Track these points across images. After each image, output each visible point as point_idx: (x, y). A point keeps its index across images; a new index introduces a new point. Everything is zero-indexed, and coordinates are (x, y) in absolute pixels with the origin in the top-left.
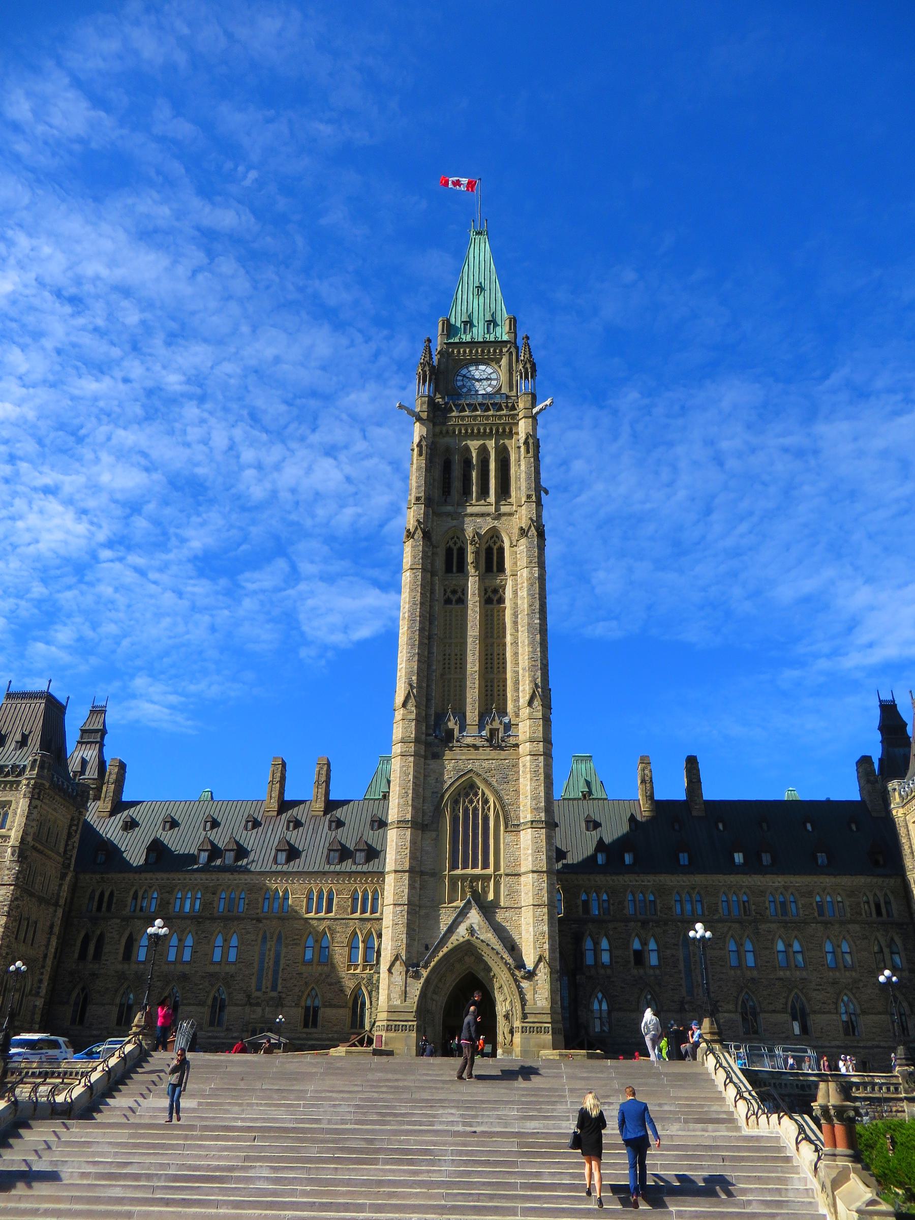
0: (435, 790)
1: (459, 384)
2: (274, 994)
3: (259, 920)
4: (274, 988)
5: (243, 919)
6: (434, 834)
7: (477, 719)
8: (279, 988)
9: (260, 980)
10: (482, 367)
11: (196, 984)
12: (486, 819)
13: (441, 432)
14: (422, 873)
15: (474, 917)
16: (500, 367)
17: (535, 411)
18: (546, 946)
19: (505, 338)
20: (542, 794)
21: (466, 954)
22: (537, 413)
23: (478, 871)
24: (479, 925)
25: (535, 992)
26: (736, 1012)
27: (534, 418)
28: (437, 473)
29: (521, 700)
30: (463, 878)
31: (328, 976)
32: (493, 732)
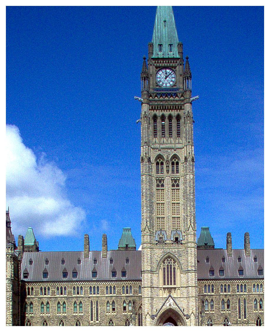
1: (159, 80)
2: (98, 322)
3: (89, 297)
4: (97, 320)
5: (83, 297)
7: (170, 234)
8: (99, 320)
9: (92, 317)
10: (168, 71)
11: (69, 319)
12: (174, 268)
13: (152, 107)
14: (153, 288)
15: (171, 301)
16: (176, 71)
17: (192, 99)
18: (194, 309)
19: (178, 56)
20: (193, 261)
22: (192, 101)
23: (173, 286)
24: (173, 303)
26: (255, 324)
27: (191, 103)
28: (151, 128)
29: (186, 227)
30: (168, 288)
31: (116, 315)
32: (177, 239)
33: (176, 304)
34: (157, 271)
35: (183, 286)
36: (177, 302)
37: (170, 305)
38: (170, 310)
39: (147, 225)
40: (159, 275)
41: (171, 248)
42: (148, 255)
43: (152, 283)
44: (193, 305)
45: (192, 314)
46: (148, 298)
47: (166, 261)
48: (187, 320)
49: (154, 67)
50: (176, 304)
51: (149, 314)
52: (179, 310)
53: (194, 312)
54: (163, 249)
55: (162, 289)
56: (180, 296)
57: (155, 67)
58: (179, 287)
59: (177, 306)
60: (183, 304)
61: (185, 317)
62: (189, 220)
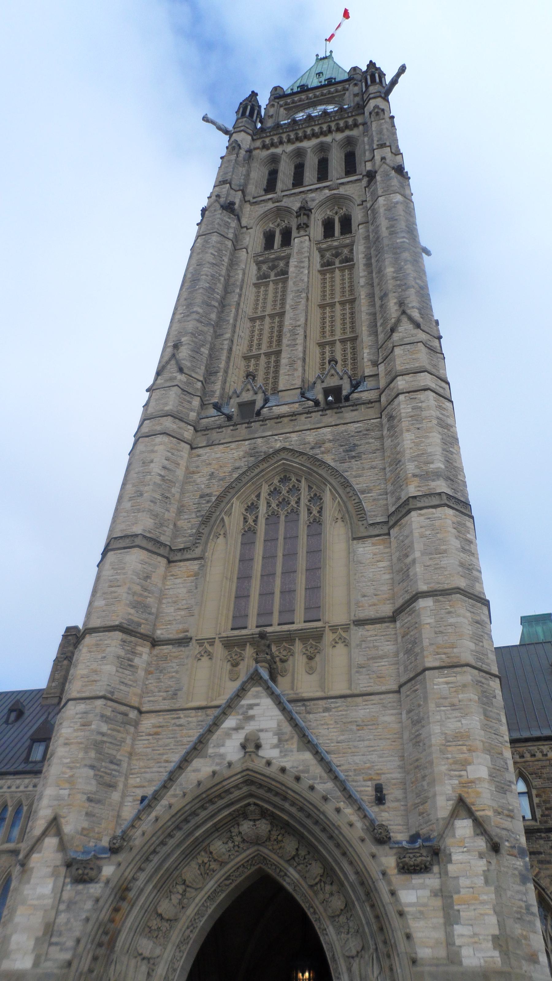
0: (208, 491)
6: (194, 566)
15: (265, 715)
18: (480, 770)
21: (243, 814)
24: (279, 733)
25: (450, 918)
33: (307, 742)
34: (198, 552)
35: (371, 613)
36: (325, 728)
37: (251, 746)
38: (259, 802)
39: (174, 355)
40: (202, 567)
41: (297, 428)
42: (152, 461)
43: (139, 605)
44: (460, 737)
45: (464, 827)
46: (82, 707)
47: (264, 495)
48: (414, 894)
49: (282, 109)
50: (307, 742)
51: (59, 833)
52: (330, 785)
53: (485, 800)
54: (247, 443)
55: (219, 650)
56: (350, 688)
57: (285, 109)
58: (346, 628)
59: (308, 756)
60: (364, 746)
61: (389, 861)
62: (395, 301)
